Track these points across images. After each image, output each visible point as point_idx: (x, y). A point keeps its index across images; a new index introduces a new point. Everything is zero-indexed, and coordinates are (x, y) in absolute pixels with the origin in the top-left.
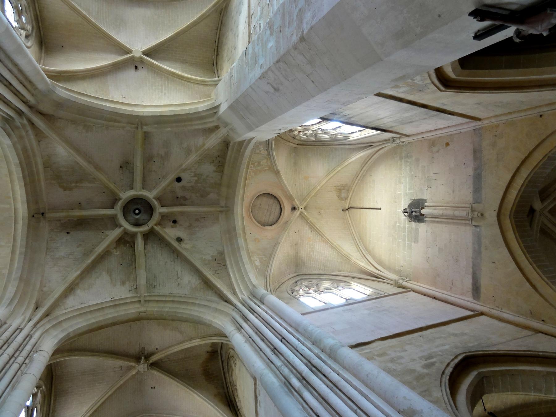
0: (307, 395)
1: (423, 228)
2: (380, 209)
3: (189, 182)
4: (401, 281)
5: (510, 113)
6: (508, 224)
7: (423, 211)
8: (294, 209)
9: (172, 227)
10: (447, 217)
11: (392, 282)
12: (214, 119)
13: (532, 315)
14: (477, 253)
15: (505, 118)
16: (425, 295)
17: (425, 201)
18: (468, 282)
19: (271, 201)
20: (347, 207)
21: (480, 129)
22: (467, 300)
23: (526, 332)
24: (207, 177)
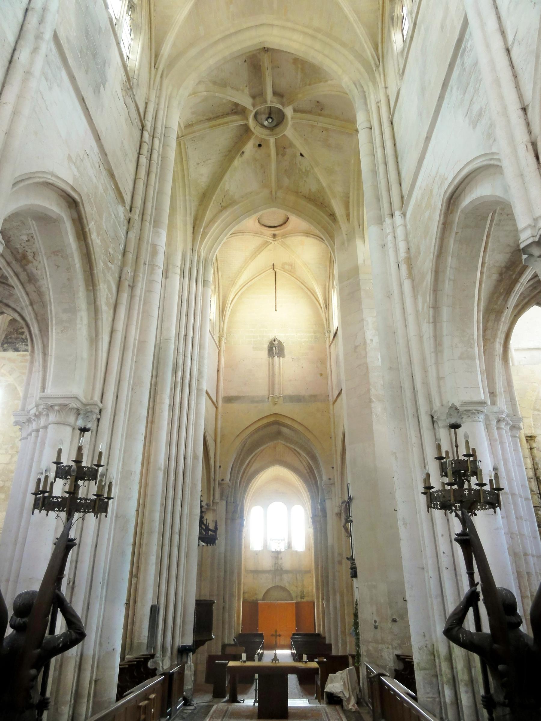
0: (178, 390)
1: (264, 354)
2: (276, 310)
3: (300, 162)
4: (223, 339)
5: (334, 423)
6: (272, 419)
7: (276, 357)
8: (274, 236)
9: (254, 145)
10: (273, 384)
11: (221, 332)
12: (356, 224)
13: (223, 436)
14: (253, 400)
15: (332, 419)
16: (218, 362)
17: (283, 357)
18: (233, 393)
19: (281, 221)
20: (275, 269)
21: (328, 401)
22: (221, 395)
23: (213, 436)
24: (305, 181)
